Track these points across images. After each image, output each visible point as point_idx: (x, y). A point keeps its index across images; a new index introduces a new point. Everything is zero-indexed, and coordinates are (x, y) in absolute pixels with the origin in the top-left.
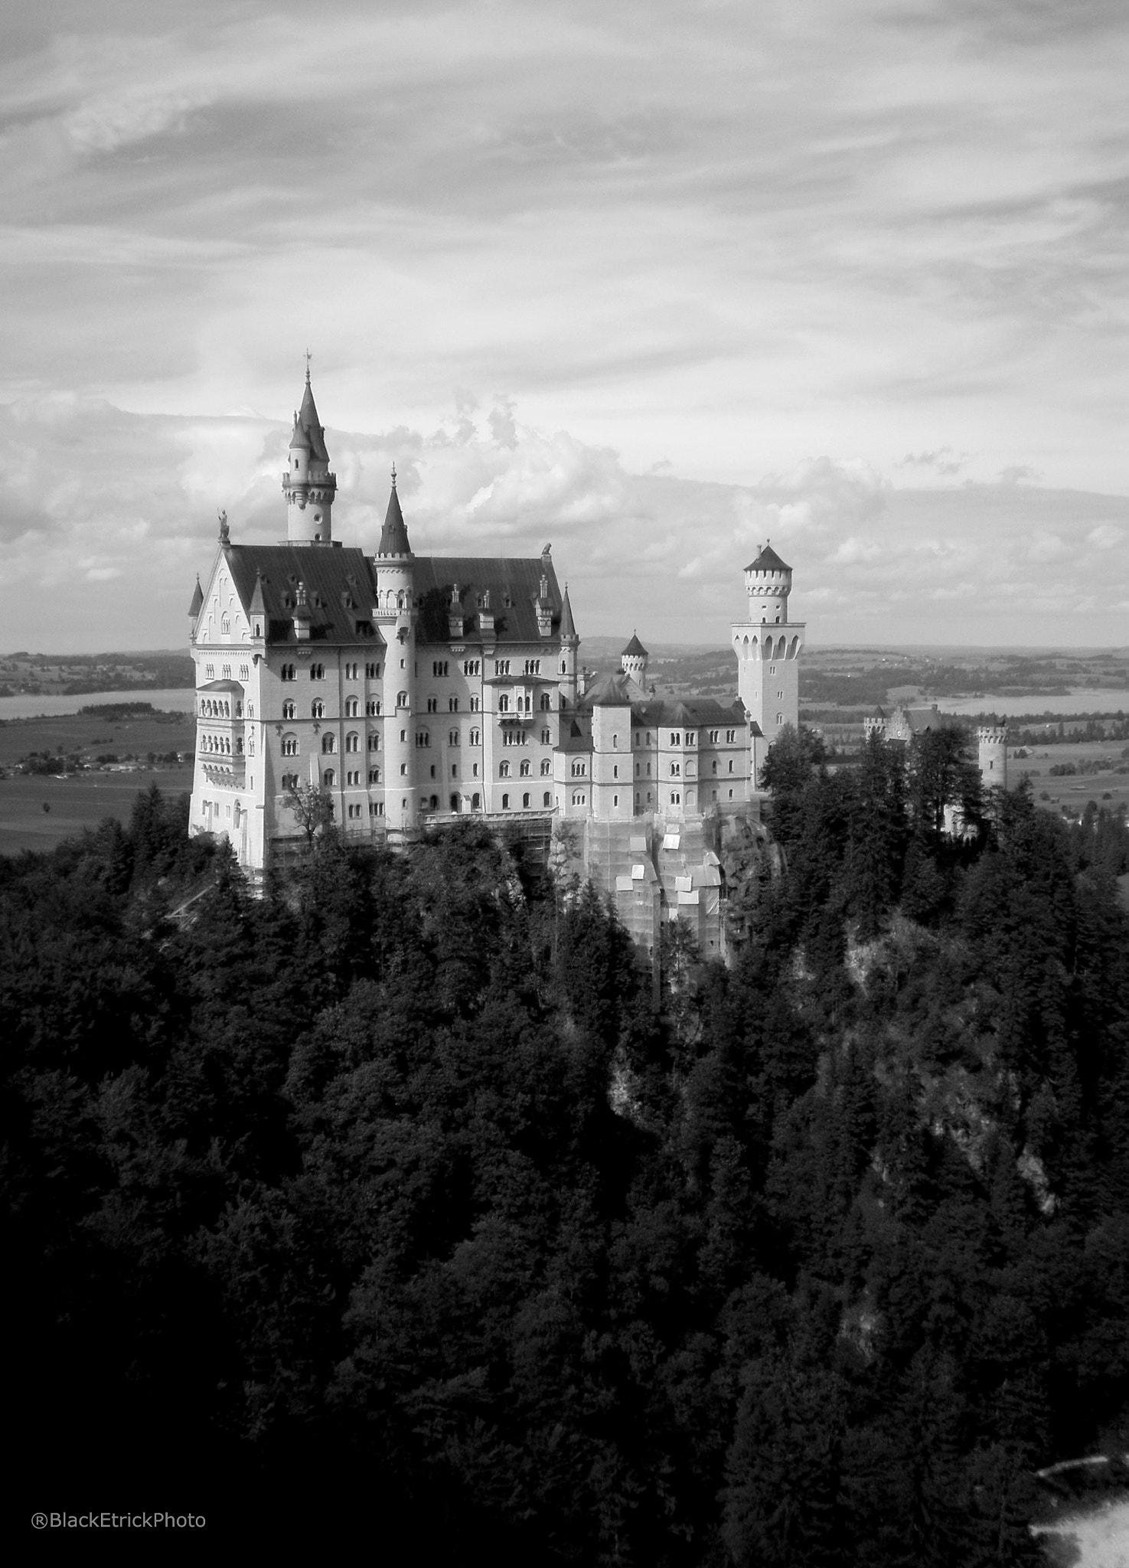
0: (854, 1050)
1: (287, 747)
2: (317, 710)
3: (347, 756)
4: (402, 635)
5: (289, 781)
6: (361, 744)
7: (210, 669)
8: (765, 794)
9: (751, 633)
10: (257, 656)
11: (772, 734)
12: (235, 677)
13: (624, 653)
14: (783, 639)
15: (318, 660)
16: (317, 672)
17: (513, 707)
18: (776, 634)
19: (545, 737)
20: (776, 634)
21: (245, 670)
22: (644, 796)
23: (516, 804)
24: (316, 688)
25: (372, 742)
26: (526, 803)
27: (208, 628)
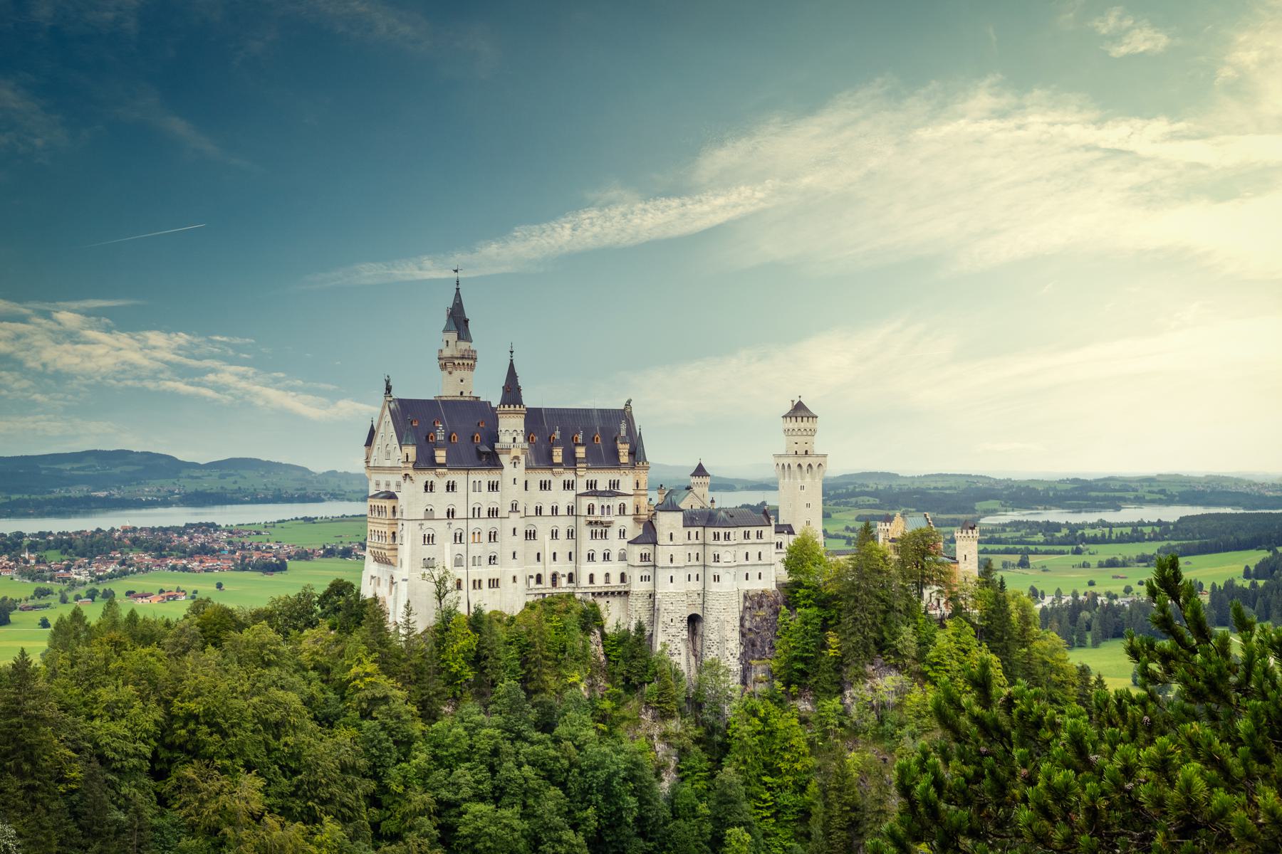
2: (451, 514)
5: (429, 564)
6: (485, 537)
7: (378, 484)
8: (785, 577)
9: (786, 461)
12: (393, 489)
17: (597, 512)
18: (805, 462)
21: (398, 485)
22: (693, 577)
23: (599, 581)
25: (493, 537)
26: (607, 582)
27: (378, 457)
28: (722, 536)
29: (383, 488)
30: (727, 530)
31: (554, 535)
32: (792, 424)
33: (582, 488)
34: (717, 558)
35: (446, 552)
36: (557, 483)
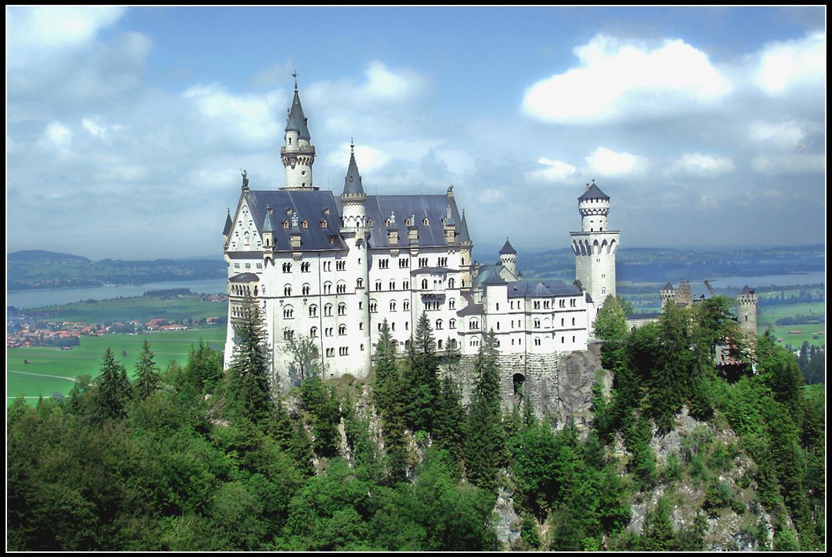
0: (660, 501)
1: (288, 313)
2: (306, 290)
3: (324, 319)
4: (359, 244)
5: (289, 334)
6: (334, 311)
10: (267, 258)
11: (599, 299)
12: (253, 270)
13: (501, 253)
14: (605, 242)
15: (305, 260)
16: (305, 267)
17: (430, 286)
18: (600, 238)
19: (452, 304)
20: (600, 238)
22: (516, 342)
24: (305, 277)
25: (341, 308)
28: (542, 304)
29: (243, 270)
30: (546, 300)
31: (392, 306)
32: (587, 205)
33: (414, 264)
34: (537, 324)
35: (301, 325)
36: (393, 262)
